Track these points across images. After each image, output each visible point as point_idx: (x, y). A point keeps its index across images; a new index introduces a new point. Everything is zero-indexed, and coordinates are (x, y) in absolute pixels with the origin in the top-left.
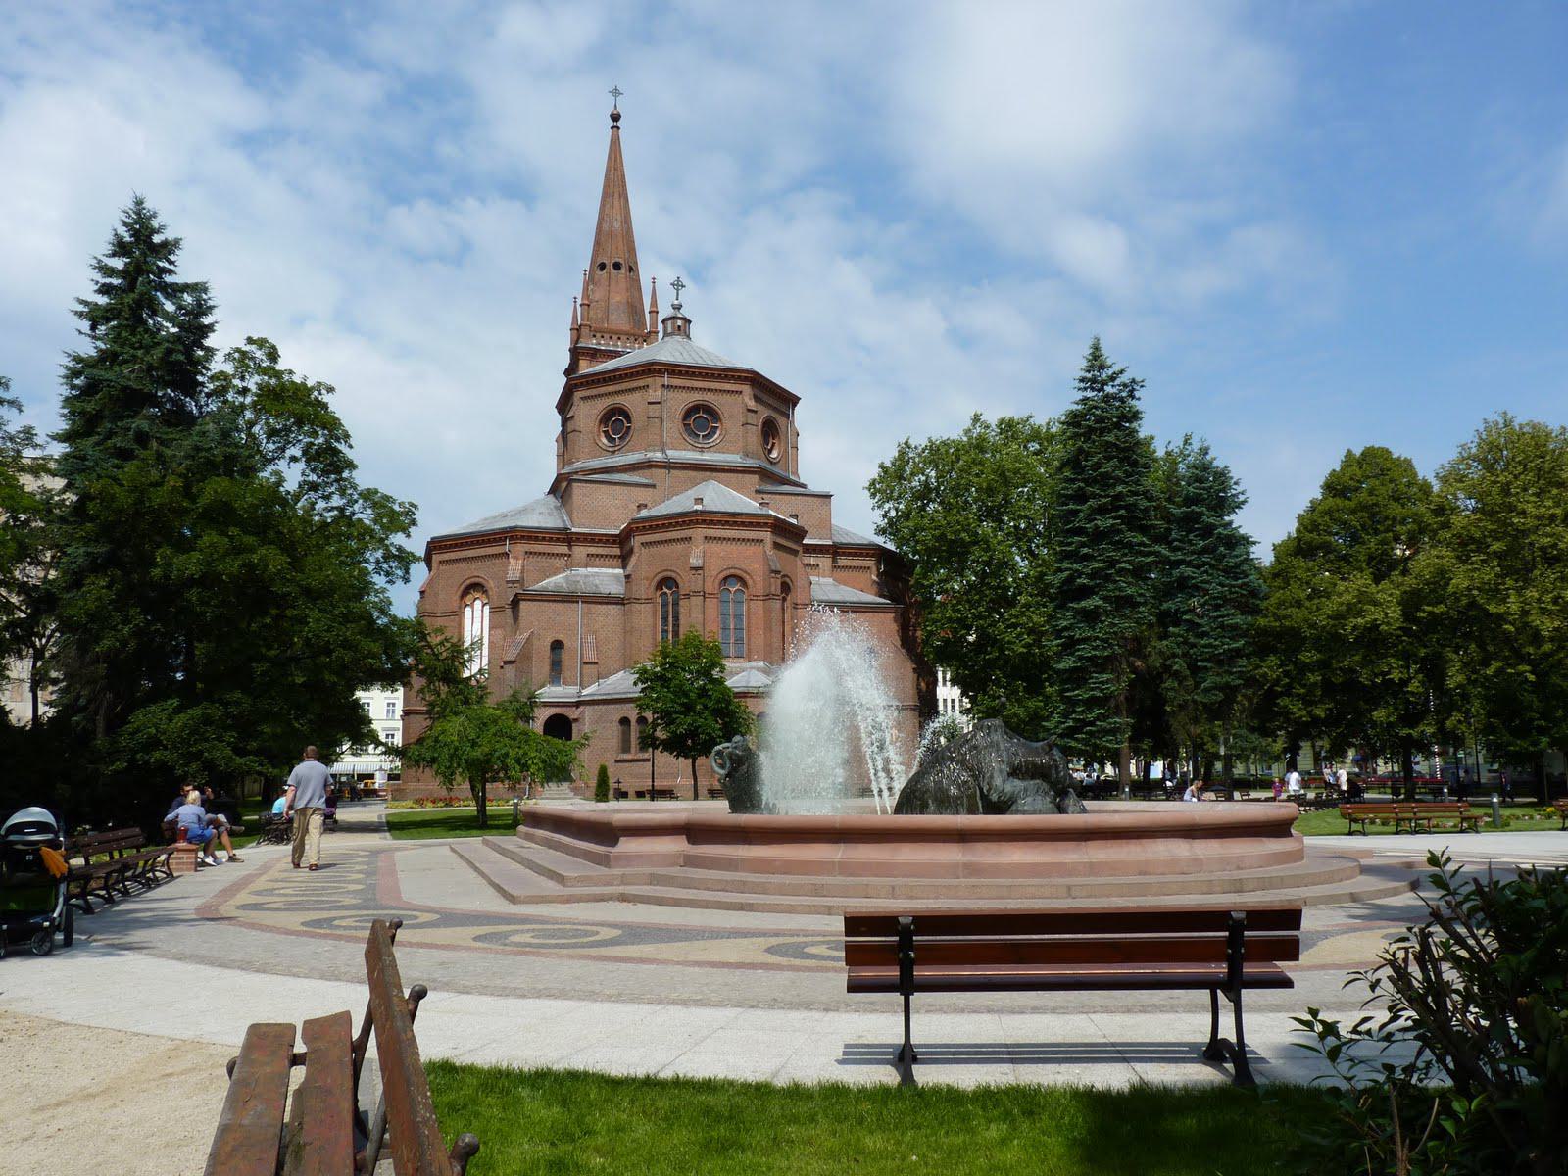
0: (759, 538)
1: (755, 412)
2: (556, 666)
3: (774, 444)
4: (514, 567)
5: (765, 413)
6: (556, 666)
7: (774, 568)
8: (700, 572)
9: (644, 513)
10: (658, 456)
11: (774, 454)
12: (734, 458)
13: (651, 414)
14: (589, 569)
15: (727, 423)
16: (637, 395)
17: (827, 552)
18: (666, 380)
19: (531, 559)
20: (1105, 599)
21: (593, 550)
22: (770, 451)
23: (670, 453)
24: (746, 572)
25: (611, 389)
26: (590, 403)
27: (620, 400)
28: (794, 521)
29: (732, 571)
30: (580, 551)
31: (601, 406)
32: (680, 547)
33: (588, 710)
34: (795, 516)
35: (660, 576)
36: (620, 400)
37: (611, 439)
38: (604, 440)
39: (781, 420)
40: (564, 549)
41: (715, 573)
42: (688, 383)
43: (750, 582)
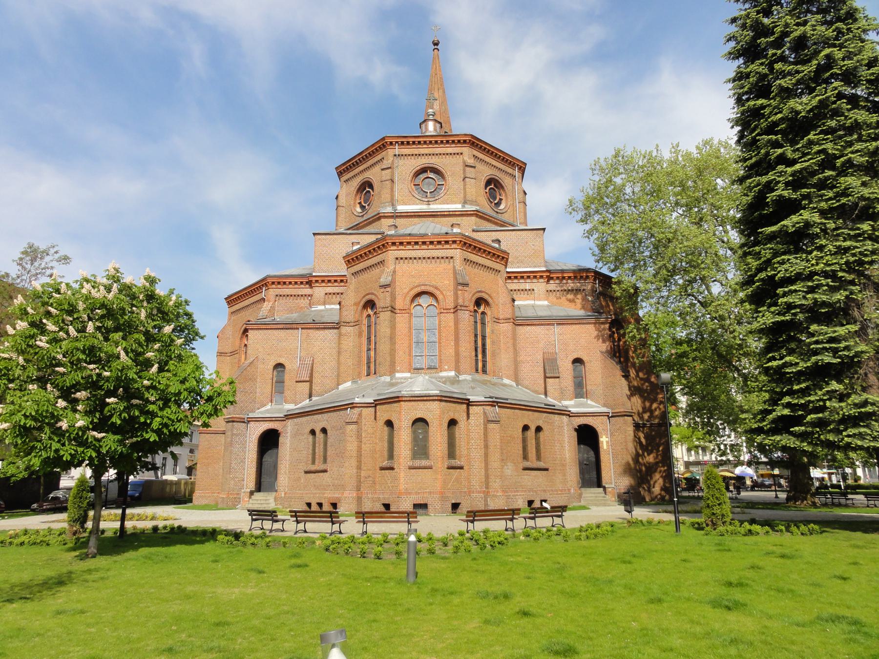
0: (449, 255)
1: (474, 167)
2: (279, 385)
3: (501, 200)
4: (266, 306)
5: (486, 172)
6: (279, 385)
7: (461, 281)
8: (388, 289)
9: (355, 248)
10: (389, 209)
11: (502, 207)
12: (458, 207)
13: (384, 179)
14: (327, 306)
15: (449, 179)
16: (377, 169)
17: (541, 277)
18: (397, 150)
19: (281, 301)
20: (823, 213)
21: (330, 290)
22: (498, 204)
23: (401, 208)
24: (436, 288)
25: (361, 168)
26: (350, 183)
27: (368, 175)
28: (497, 245)
29: (423, 288)
30: (319, 291)
31: (356, 183)
32: (376, 271)
33: (290, 423)
34: (499, 241)
35: (364, 300)
36: (368, 175)
37: (363, 207)
38: (359, 210)
39: (506, 181)
40: (308, 291)
41: (405, 291)
42: (416, 151)
43: (440, 297)
